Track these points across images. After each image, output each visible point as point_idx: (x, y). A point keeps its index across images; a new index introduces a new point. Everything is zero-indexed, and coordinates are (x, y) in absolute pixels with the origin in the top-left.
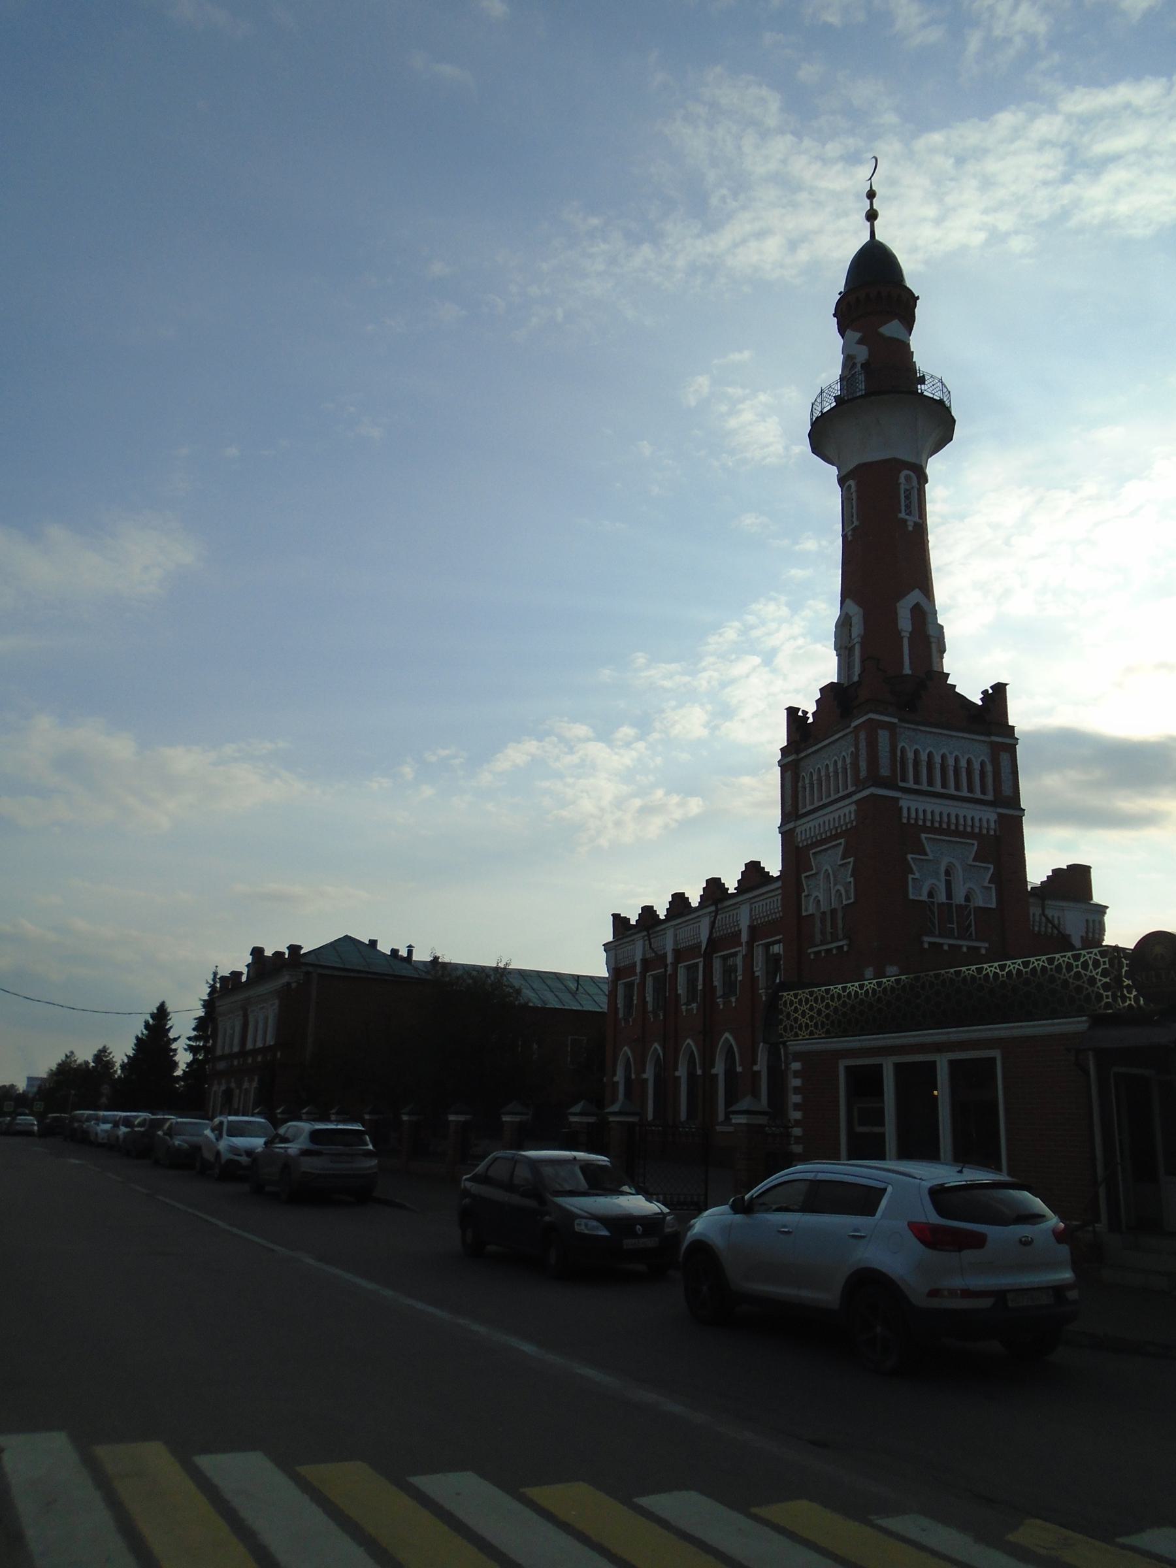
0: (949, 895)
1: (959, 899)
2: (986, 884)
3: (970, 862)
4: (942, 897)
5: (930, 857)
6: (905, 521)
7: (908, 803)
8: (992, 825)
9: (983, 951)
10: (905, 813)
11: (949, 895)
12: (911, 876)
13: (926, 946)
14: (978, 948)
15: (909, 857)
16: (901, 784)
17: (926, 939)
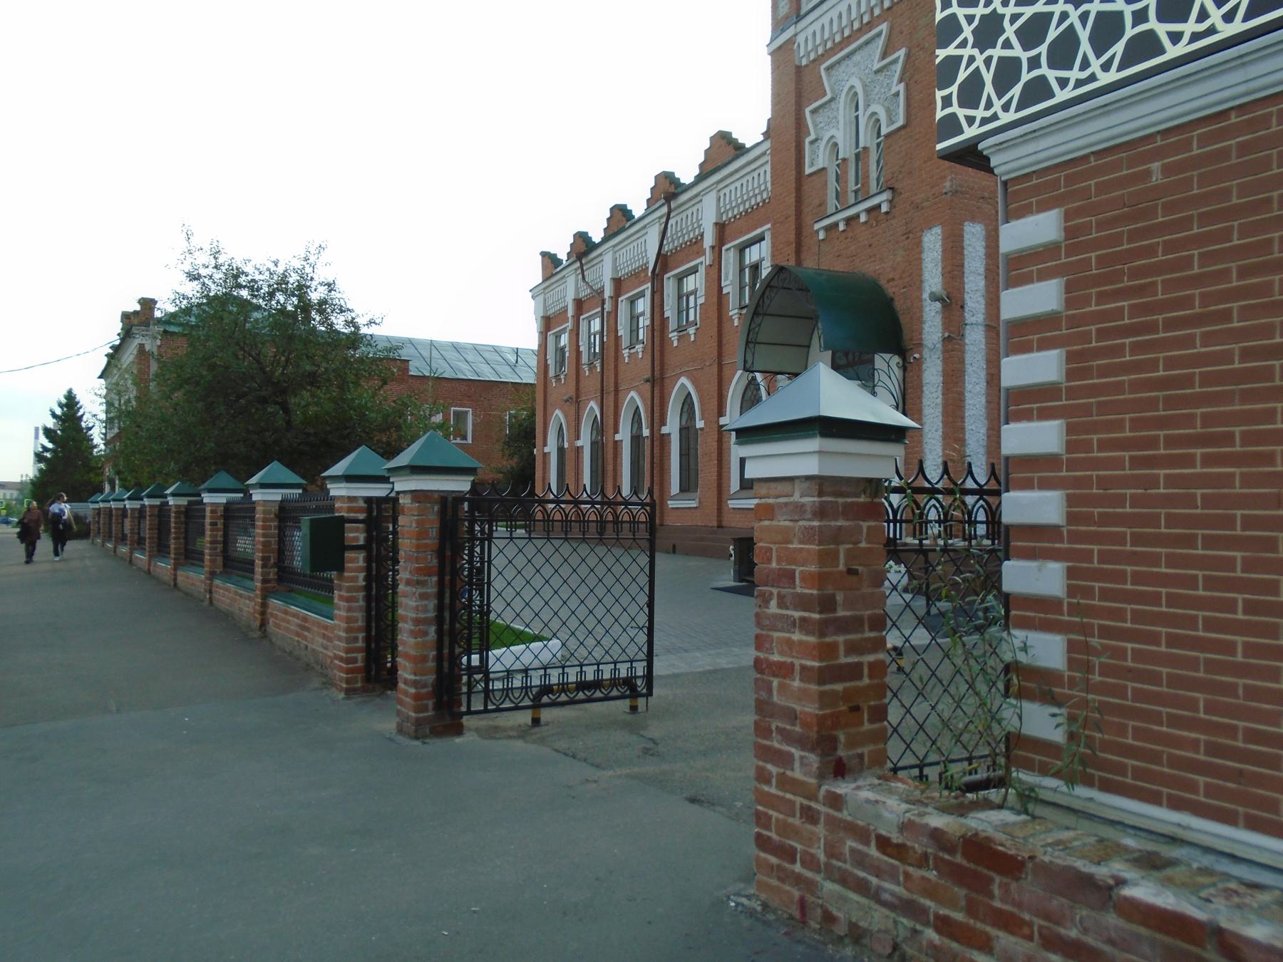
2: (894, 91)
3: (877, 66)
9: (884, 208)
12: (807, 140)
13: (822, 236)
14: (879, 206)
16: (803, 12)
17: (817, 227)
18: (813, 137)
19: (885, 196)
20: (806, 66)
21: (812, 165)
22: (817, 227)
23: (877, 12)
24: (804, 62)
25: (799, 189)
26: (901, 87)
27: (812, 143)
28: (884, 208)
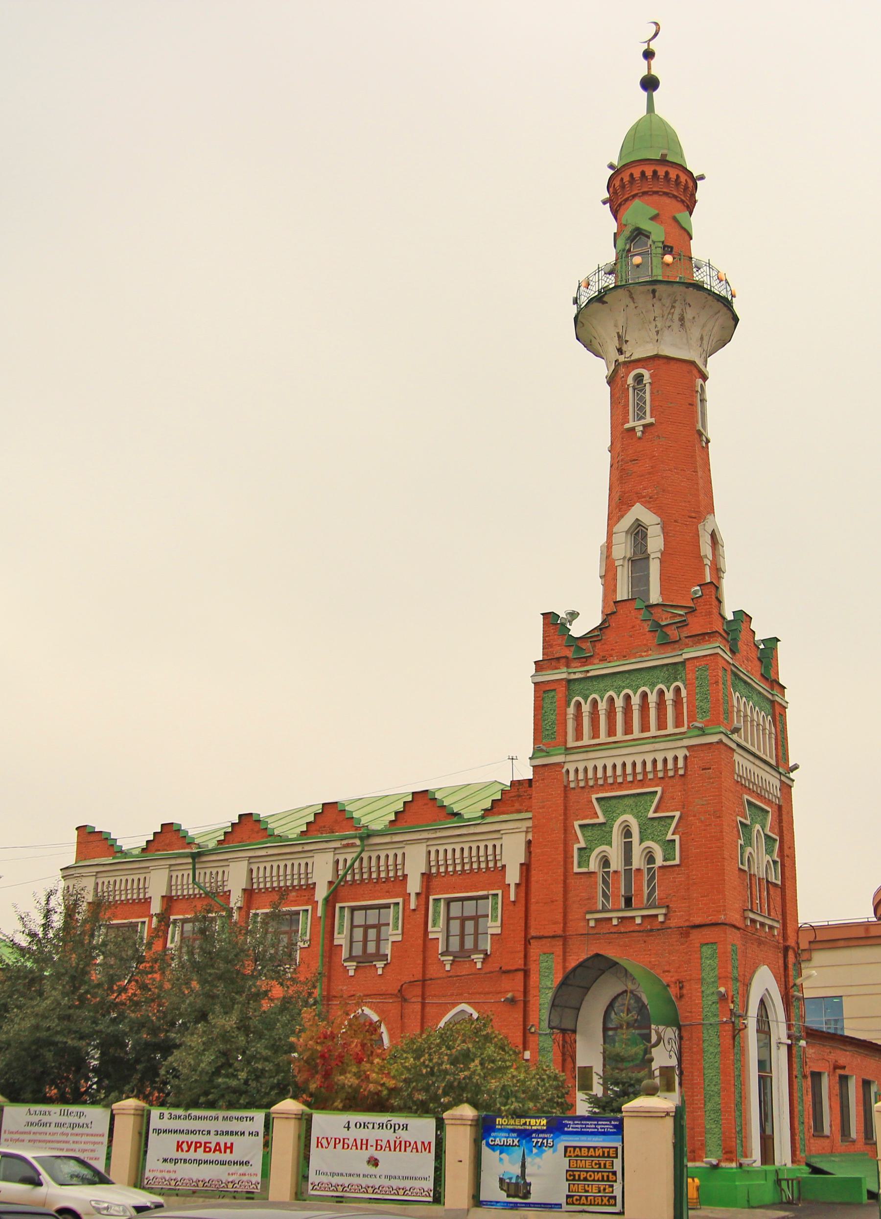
0: (628, 859)
1: (638, 861)
2: (670, 837)
3: (651, 815)
4: (616, 863)
5: (601, 819)
6: (633, 429)
7: (574, 764)
8: (681, 763)
9: (661, 918)
10: (572, 776)
11: (628, 859)
12: (576, 846)
13: (592, 923)
14: (656, 916)
15: (576, 824)
16: (571, 743)
17: (588, 916)
18: (582, 844)
19: (664, 911)
20: (574, 788)
21: (579, 866)
22: (588, 916)
23: (650, 776)
24: (572, 785)
25: (565, 882)
26: (677, 837)
27: (580, 849)
28: (661, 918)
